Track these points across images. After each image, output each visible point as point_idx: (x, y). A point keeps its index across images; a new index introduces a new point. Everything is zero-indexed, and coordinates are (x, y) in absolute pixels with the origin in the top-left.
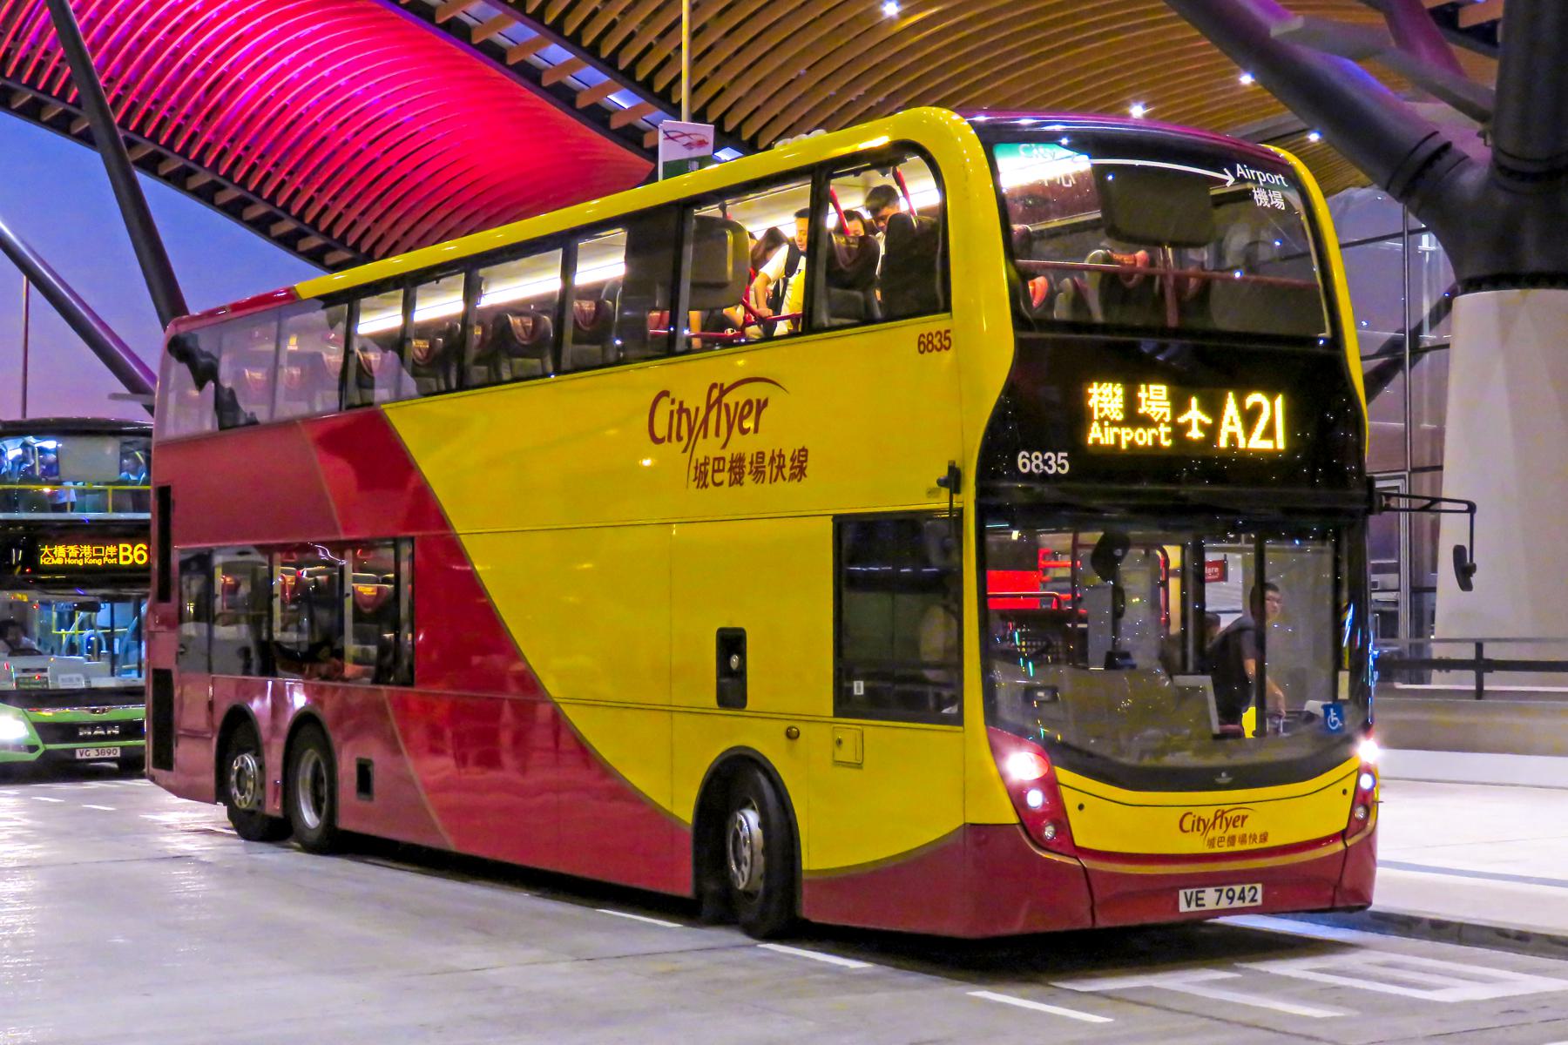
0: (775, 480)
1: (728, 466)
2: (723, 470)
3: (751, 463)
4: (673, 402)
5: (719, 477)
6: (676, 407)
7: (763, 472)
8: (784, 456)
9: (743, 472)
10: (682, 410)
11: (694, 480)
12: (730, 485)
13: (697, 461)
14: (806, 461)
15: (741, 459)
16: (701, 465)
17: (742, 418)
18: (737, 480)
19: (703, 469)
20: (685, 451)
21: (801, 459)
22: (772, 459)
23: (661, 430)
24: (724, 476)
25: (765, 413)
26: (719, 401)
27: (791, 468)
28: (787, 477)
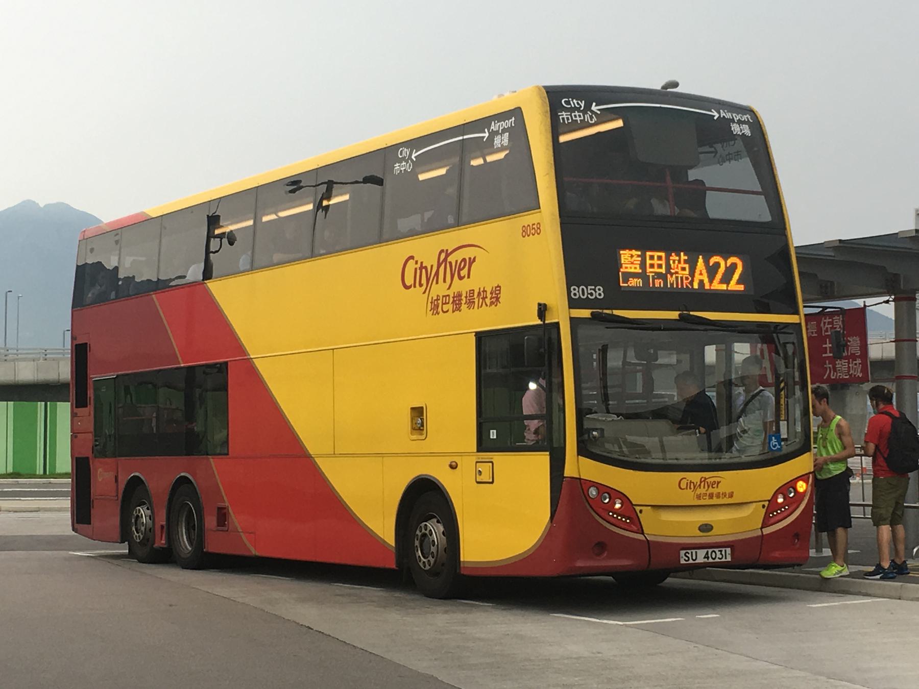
0: (481, 307)
1: (451, 300)
2: (448, 303)
3: (466, 297)
4: (416, 262)
5: (445, 308)
6: (419, 265)
7: (474, 302)
8: (486, 291)
9: (461, 303)
10: (422, 267)
11: (430, 311)
12: (453, 312)
13: (432, 298)
14: (500, 293)
15: (460, 295)
16: (435, 300)
17: (460, 270)
18: (457, 308)
19: (436, 302)
20: (424, 292)
21: (497, 292)
22: (479, 294)
23: (409, 281)
24: (449, 307)
25: (474, 263)
26: (445, 259)
27: (491, 299)
28: (488, 304)
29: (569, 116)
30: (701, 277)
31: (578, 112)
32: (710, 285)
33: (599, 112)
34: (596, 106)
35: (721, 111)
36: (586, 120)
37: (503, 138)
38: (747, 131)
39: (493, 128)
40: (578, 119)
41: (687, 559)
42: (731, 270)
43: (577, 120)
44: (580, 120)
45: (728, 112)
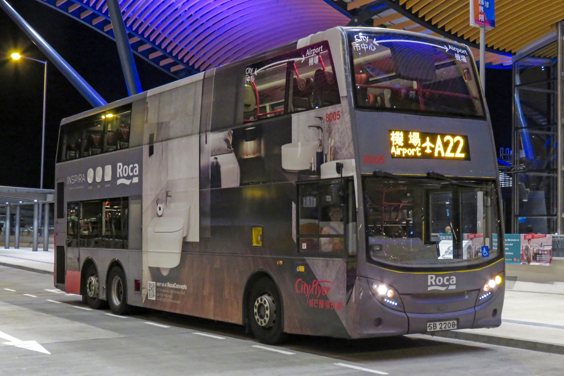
29: (359, 46)
30: (439, 149)
31: (365, 44)
32: (445, 154)
33: (378, 45)
34: (376, 41)
35: (449, 46)
36: (370, 49)
37: (315, 59)
38: (464, 59)
39: (308, 53)
40: (365, 48)
41: (430, 328)
42: (456, 144)
43: (364, 49)
44: (366, 49)
45: (453, 47)
